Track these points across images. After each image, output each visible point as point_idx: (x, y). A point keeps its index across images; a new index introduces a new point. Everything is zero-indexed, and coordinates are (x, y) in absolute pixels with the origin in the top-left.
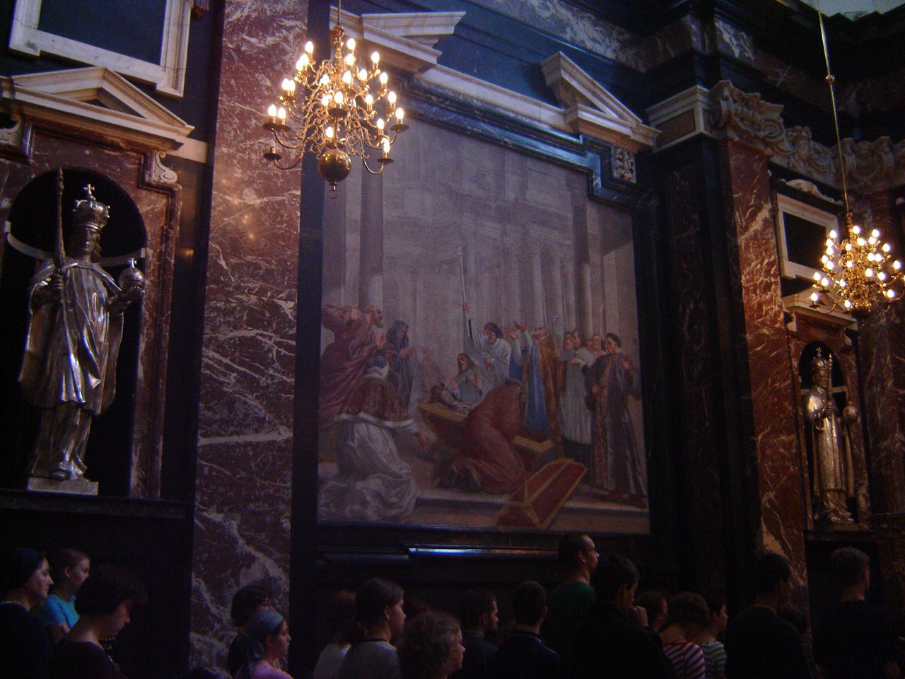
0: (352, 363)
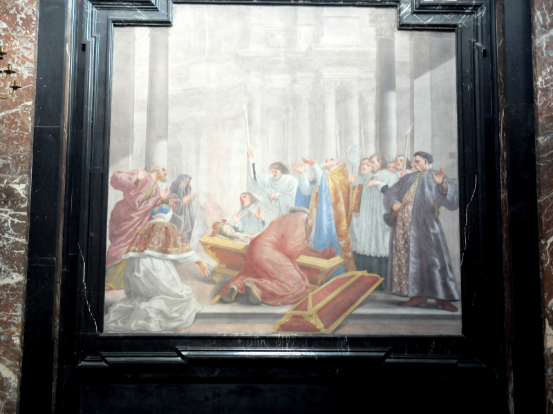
0: (137, 213)
